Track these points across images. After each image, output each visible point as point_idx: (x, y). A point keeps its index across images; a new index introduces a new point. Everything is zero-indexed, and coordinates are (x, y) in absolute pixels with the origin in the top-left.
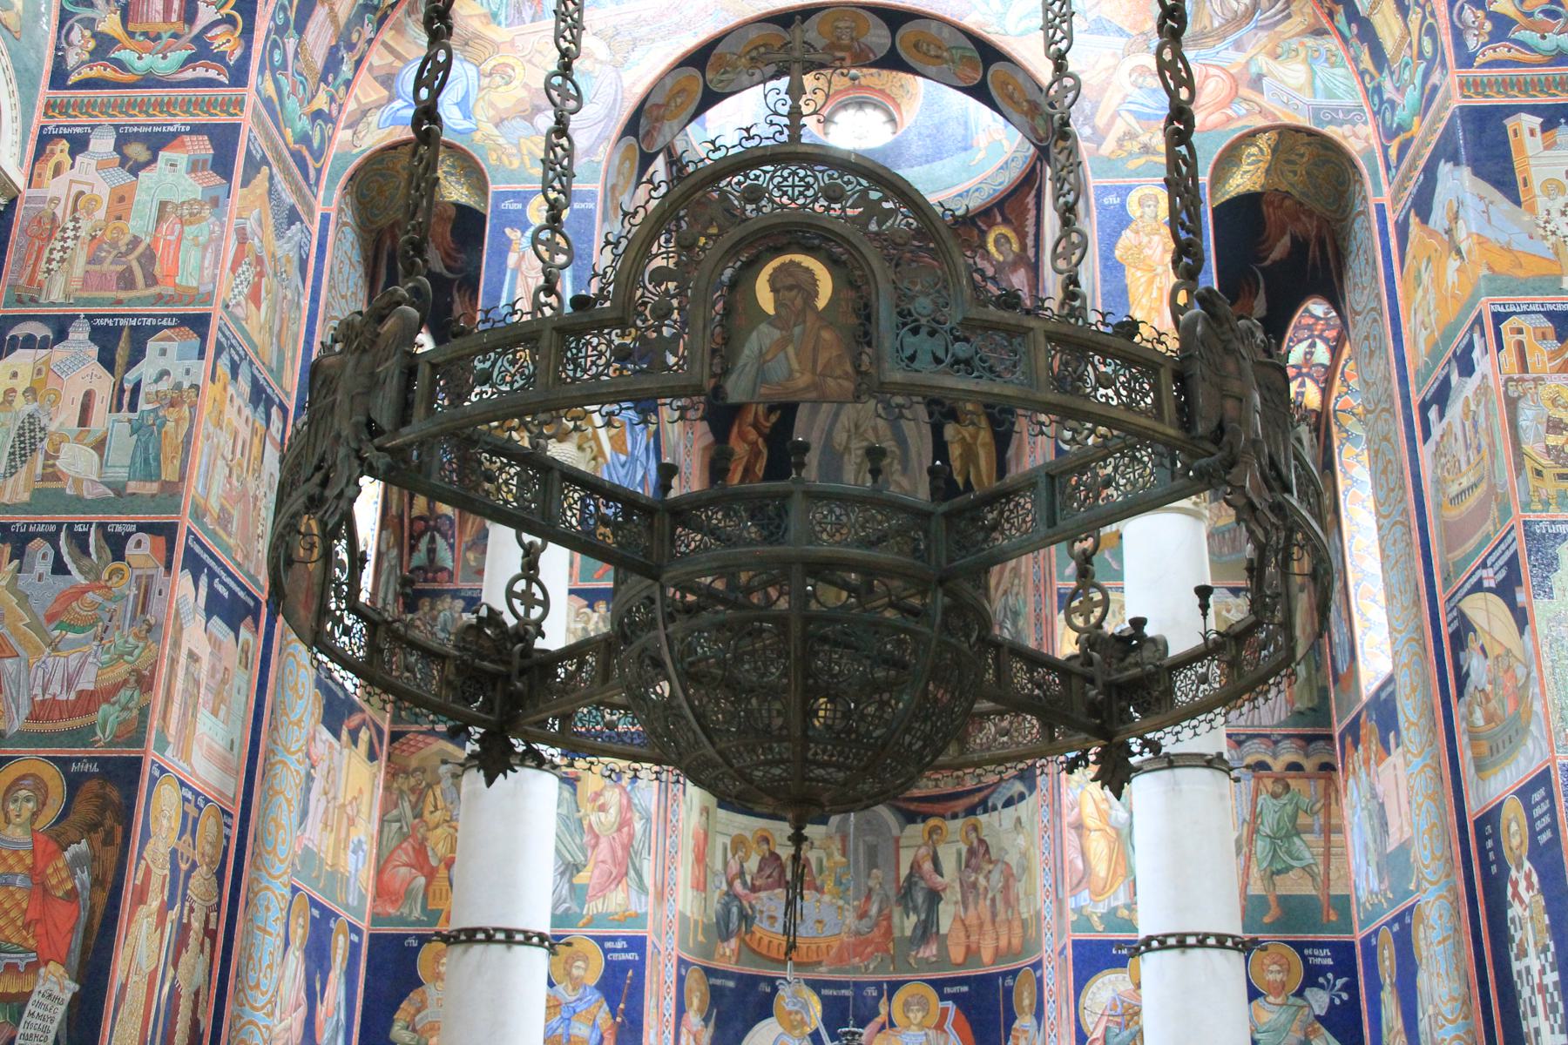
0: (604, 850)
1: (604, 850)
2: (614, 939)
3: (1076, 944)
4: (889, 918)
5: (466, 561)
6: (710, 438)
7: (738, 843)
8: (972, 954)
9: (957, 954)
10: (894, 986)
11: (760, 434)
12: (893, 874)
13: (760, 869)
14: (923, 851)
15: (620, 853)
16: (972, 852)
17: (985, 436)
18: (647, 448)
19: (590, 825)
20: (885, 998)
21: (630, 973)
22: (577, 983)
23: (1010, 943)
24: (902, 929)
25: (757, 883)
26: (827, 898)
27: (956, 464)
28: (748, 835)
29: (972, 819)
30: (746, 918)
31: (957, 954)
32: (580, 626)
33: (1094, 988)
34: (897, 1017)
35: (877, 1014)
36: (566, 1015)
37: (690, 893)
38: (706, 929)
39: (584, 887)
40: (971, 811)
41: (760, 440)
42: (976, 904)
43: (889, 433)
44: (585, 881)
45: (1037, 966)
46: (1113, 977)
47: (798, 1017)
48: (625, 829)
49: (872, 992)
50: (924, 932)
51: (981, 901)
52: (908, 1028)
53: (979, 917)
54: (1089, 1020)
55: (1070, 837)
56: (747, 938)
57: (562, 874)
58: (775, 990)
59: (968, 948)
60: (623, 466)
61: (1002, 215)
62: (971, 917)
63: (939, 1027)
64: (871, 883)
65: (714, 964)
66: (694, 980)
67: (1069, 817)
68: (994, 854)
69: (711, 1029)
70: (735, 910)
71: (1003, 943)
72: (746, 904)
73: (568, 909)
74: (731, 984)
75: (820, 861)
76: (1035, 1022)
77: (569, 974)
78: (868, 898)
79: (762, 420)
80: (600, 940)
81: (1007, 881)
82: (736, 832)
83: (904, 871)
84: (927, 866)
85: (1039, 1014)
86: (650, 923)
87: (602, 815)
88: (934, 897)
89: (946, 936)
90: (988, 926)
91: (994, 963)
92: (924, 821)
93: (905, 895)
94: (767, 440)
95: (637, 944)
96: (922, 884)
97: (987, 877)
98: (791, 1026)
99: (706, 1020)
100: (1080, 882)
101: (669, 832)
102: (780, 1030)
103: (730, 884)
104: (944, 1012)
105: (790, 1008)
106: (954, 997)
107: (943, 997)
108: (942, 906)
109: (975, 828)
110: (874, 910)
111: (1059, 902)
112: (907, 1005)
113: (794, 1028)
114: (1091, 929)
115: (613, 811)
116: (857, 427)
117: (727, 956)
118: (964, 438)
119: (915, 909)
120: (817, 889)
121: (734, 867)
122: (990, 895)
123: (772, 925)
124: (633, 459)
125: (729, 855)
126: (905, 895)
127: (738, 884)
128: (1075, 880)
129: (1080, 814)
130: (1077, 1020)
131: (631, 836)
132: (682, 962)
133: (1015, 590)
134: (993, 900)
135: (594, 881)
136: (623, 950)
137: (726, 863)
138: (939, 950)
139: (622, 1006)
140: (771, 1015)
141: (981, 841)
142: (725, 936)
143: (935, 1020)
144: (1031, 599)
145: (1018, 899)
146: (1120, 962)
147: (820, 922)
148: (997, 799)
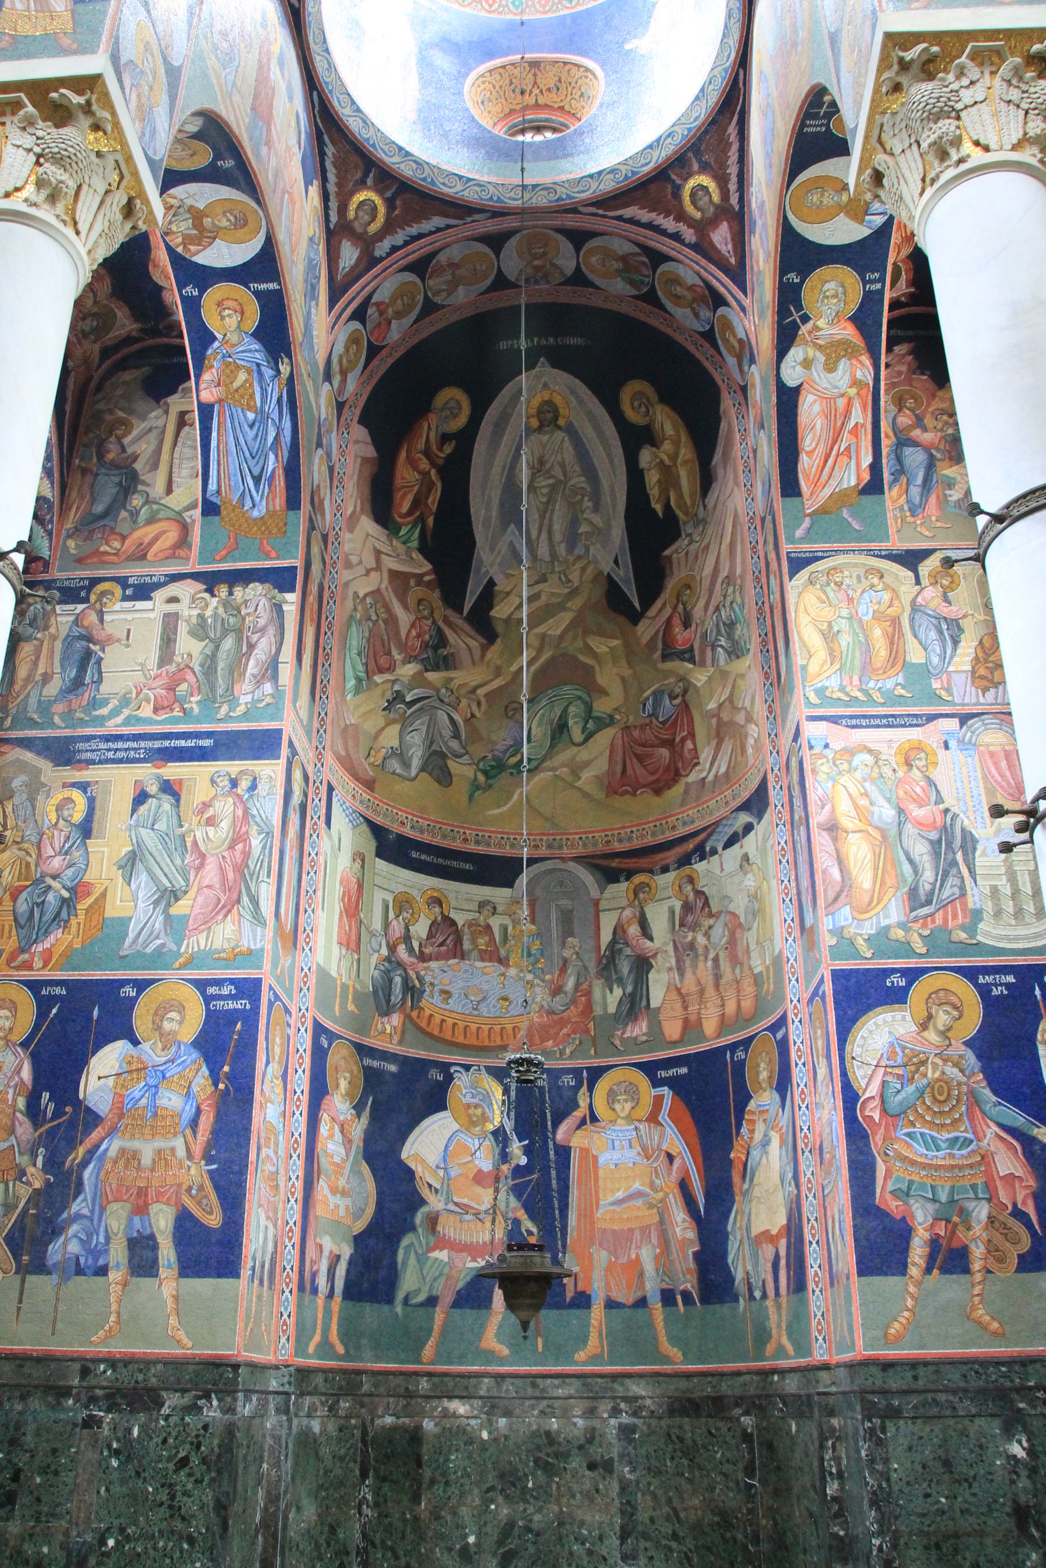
0: (210, 873)
1: (210, 873)
2: (219, 983)
3: (838, 976)
4: (588, 993)
5: (66, 548)
6: (371, 452)
7: (403, 903)
8: (691, 1027)
9: (672, 1029)
10: (596, 1074)
11: (433, 464)
12: (592, 943)
13: (431, 935)
14: (628, 913)
15: (231, 875)
16: (687, 908)
17: (687, 452)
18: (279, 401)
19: (195, 843)
20: (585, 1087)
21: (239, 1026)
22: (168, 1040)
23: (739, 1007)
24: (605, 1005)
25: (427, 951)
26: (512, 972)
27: (654, 492)
28: (415, 893)
29: (686, 870)
30: (413, 992)
31: (672, 1029)
32: (195, 612)
33: (864, 1032)
34: (601, 1109)
35: (577, 1106)
36: (152, 1082)
37: (336, 950)
38: (359, 998)
39: (184, 919)
40: (685, 861)
41: (433, 472)
42: (695, 967)
43: (577, 468)
44: (186, 911)
45: (782, 1022)
46: (888, 1016)
47: (479, 1112)
48: (239, 847)
49: (568, 1080)
50: (632, 1008)
51: (701, 965)
52: (613, 1122)
53: (699, 983)
54: (859, 1073)
55: (821, 841)
56: (414, 1014)
57: (156, 903)
58: (449, 1078)
59: (686, 1021)
60: (251, 426)
61: (700, 161)
62: (689, 983)
63: (653, 1118)
64: (566, 953)
65: (367, 1041)
66: (339, 1056)
67: (818, 817)
68: (715, 906)
69: (365, 1120)
70: (398, 980)
71: (731, 1008)
72: (412, 974)
73: (163, 945)
74: (393, 1068)
75: (504, 929)
76: (777, 1097)
77: (159, 1028)
78: (563, 970)
79: (434, 448)
80: (201, 985)
81: (732, 934)
82: (400, 889)
83: (606, 937)
84: (634, 930)
85: (783, 1083)
86: (267, 965)
87: (211, 830)
88: (643, 965)
89: (658, 1009)
90: (710, 992)
91: (718, 1036)
92: (627, 879)
93: (608, 966)
94: (442, 471)
95: (250, 989)
96: (628, 951)
98: (471, 1122)
99: (358, 1108)
100: (836, 899)
101: (306, 866)
102: (456, 1126)
103: (392, 948)
104: (658, 1101)
105: (468, 1100)
106: (672, 1083)
107: (656, 1083)
108: (651, 975)
109: (691, 880)
110: (570, 984)
111: (807, 933)
112: (612, 1096)
113: (474, 1124)
114: (857, 955)
115: (225, 825)
116: (542, 462)
117: (388, 1033)
118: (662, 462)
119: (620, 982)
120: (500, 961)
121: (397, 928)
122: (711, 955)
123: (446, 1001)
124: (263, 417)
125: (391, 915)
126: (608, 966)
127: (402, 950)
128: (831, 895)
129: (833, 810)
130: (844, 1074)
131: (247, 855)
132: (319, 1029)
133: (729, 599)
134: (716, 960)
135: (196, 911)
136: (231, 997)
137: (386, 924)
138: (649, 1026)
139: (226, 1069)
140: (444, 1108)
141: (699, 893)
142: (386, 1010)
143: (645, 1110)
144: (750, 592)
145: (748, 951)
146: (898, 997)
147: (505, 999)
148: (718, 841)
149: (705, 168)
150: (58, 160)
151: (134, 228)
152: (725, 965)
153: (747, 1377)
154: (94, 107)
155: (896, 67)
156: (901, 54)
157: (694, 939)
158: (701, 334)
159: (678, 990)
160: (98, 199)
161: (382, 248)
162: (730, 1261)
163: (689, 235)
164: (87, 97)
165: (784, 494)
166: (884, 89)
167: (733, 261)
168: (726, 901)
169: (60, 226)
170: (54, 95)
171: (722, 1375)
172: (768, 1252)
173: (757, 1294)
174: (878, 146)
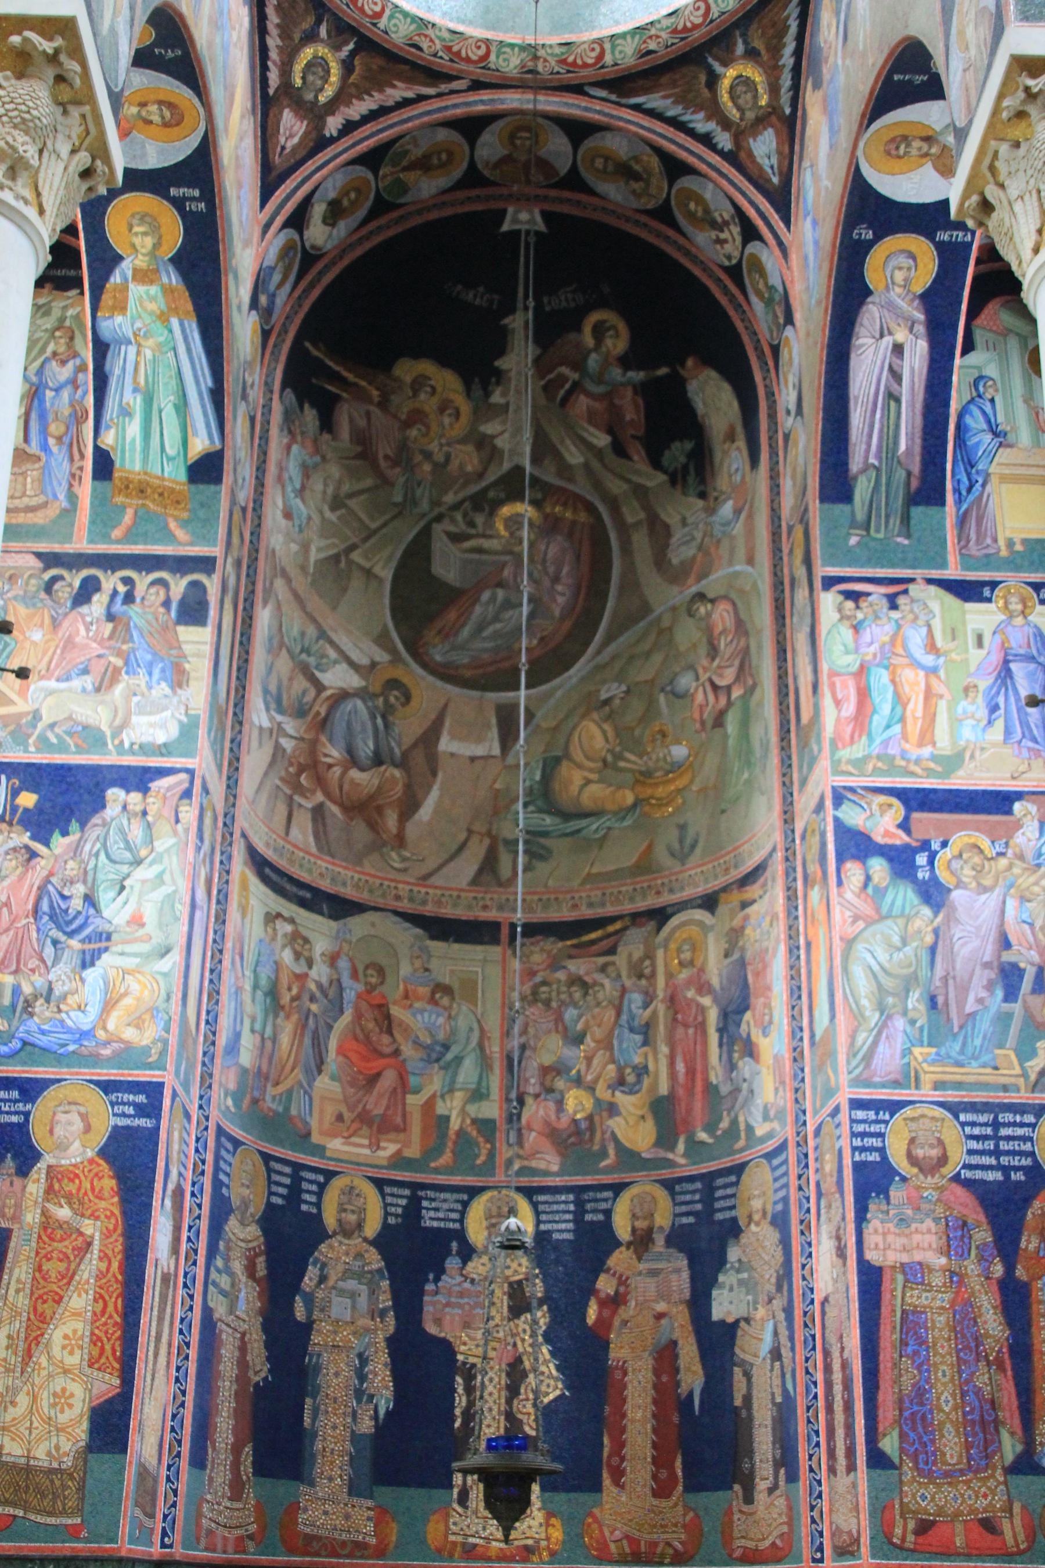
149: (752, 54)
150: (24, 125)
151: (90, 189)
154: (63, 58)
155: (1021, 95)
156: (1030, 82)
158: (726, 270)
160: (62, 166)
161: (333, 124)
163: (724, 140)
164: (55, 44)
165: (825, 497)
166: (1005, 115)
167: (775, 180)
169: (20, 205)
170: (15, 39)
174: (988, 175)
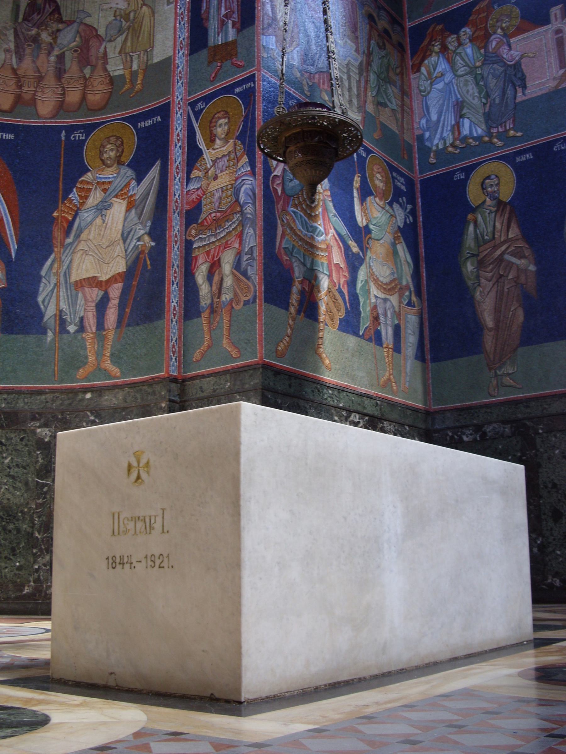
51: (43, 57)
68: (66, 15)
71: (73, 97)
90: (50, 80)
91: (53, 117)
97: (55, 35)
122: (56, 52)
134: (61, 58)
152: (71, 64)
153: (49, 396)
157: (38, 35)
159: (14, 71)
162: (40, 299)
168: (82, 15)
171: (19, 392)
172: (96, 294)
173: (72, 328)
